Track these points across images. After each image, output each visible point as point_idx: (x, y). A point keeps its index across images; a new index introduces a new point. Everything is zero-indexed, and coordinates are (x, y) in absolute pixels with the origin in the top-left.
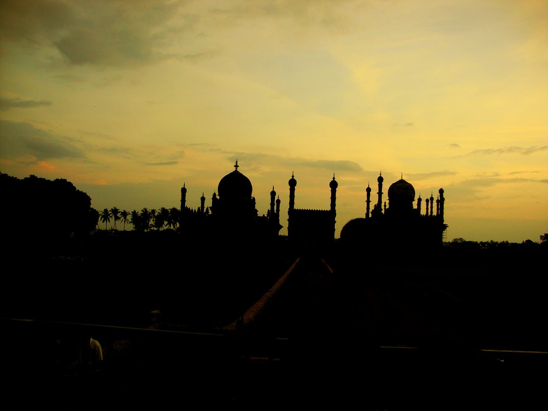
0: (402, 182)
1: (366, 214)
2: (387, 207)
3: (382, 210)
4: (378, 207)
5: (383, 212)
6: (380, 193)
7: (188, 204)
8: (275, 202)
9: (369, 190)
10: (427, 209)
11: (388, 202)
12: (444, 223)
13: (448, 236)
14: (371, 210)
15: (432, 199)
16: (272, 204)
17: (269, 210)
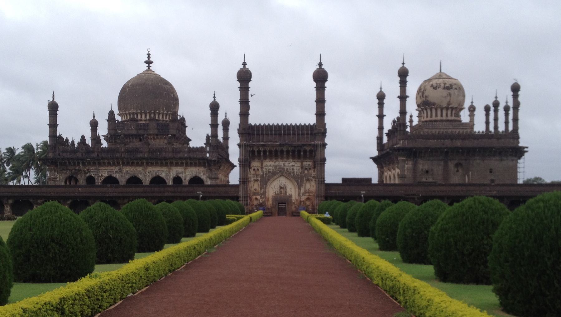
0: (440, 76)
1: (378, 138)
2: (416, 122)
3: (406, 127)
4: (399, 124)
5: (408, 129)
6: (403, 98)
7: (60, 131)
8: (220, 121)
9: (381, 97)
10: (487, 123)
11: (415, 114)
12: (521, 145)
13: (527, 170)
14: (385, 131)
15: (496, 105)
16: (214, 126)
17: (208, 137)
